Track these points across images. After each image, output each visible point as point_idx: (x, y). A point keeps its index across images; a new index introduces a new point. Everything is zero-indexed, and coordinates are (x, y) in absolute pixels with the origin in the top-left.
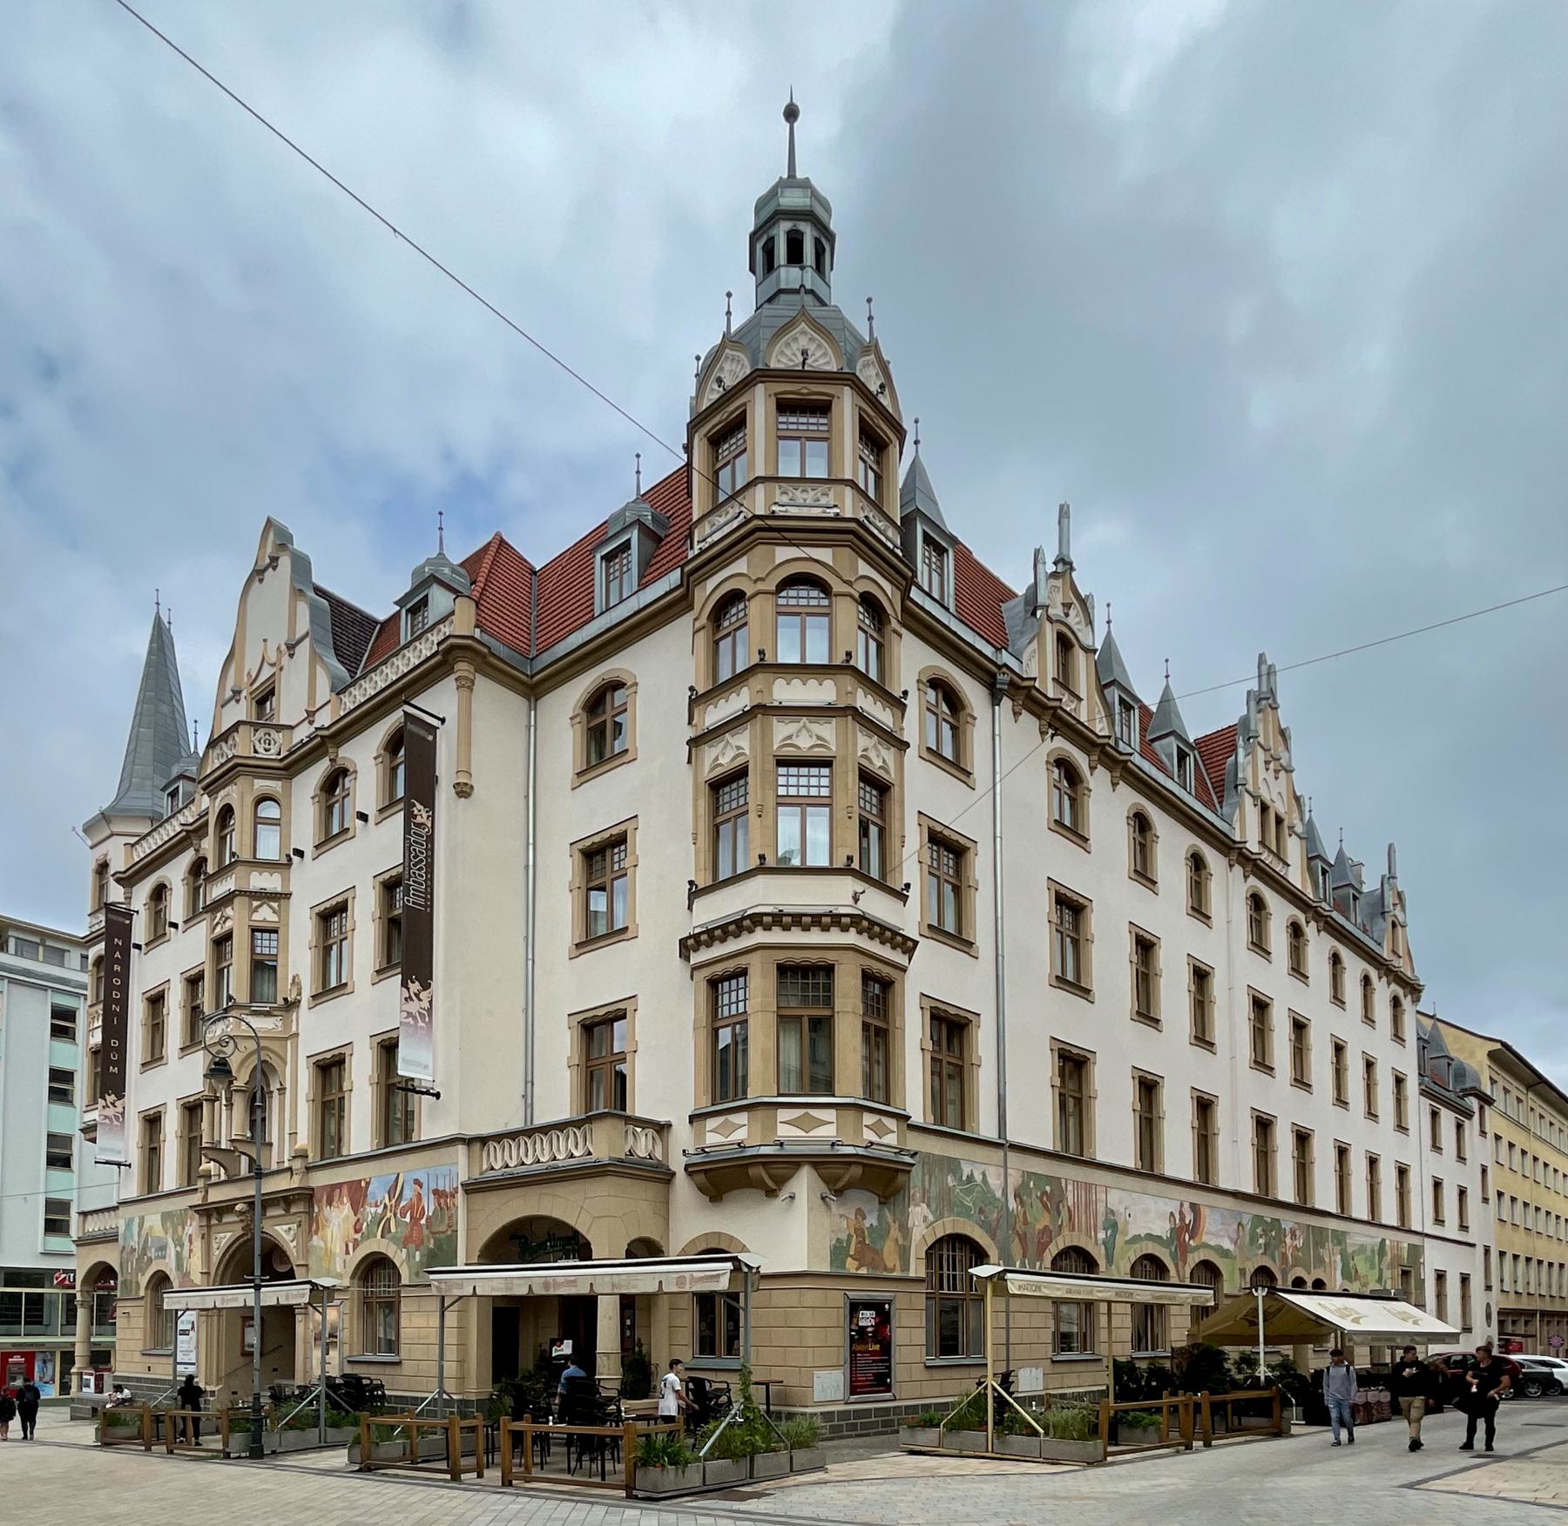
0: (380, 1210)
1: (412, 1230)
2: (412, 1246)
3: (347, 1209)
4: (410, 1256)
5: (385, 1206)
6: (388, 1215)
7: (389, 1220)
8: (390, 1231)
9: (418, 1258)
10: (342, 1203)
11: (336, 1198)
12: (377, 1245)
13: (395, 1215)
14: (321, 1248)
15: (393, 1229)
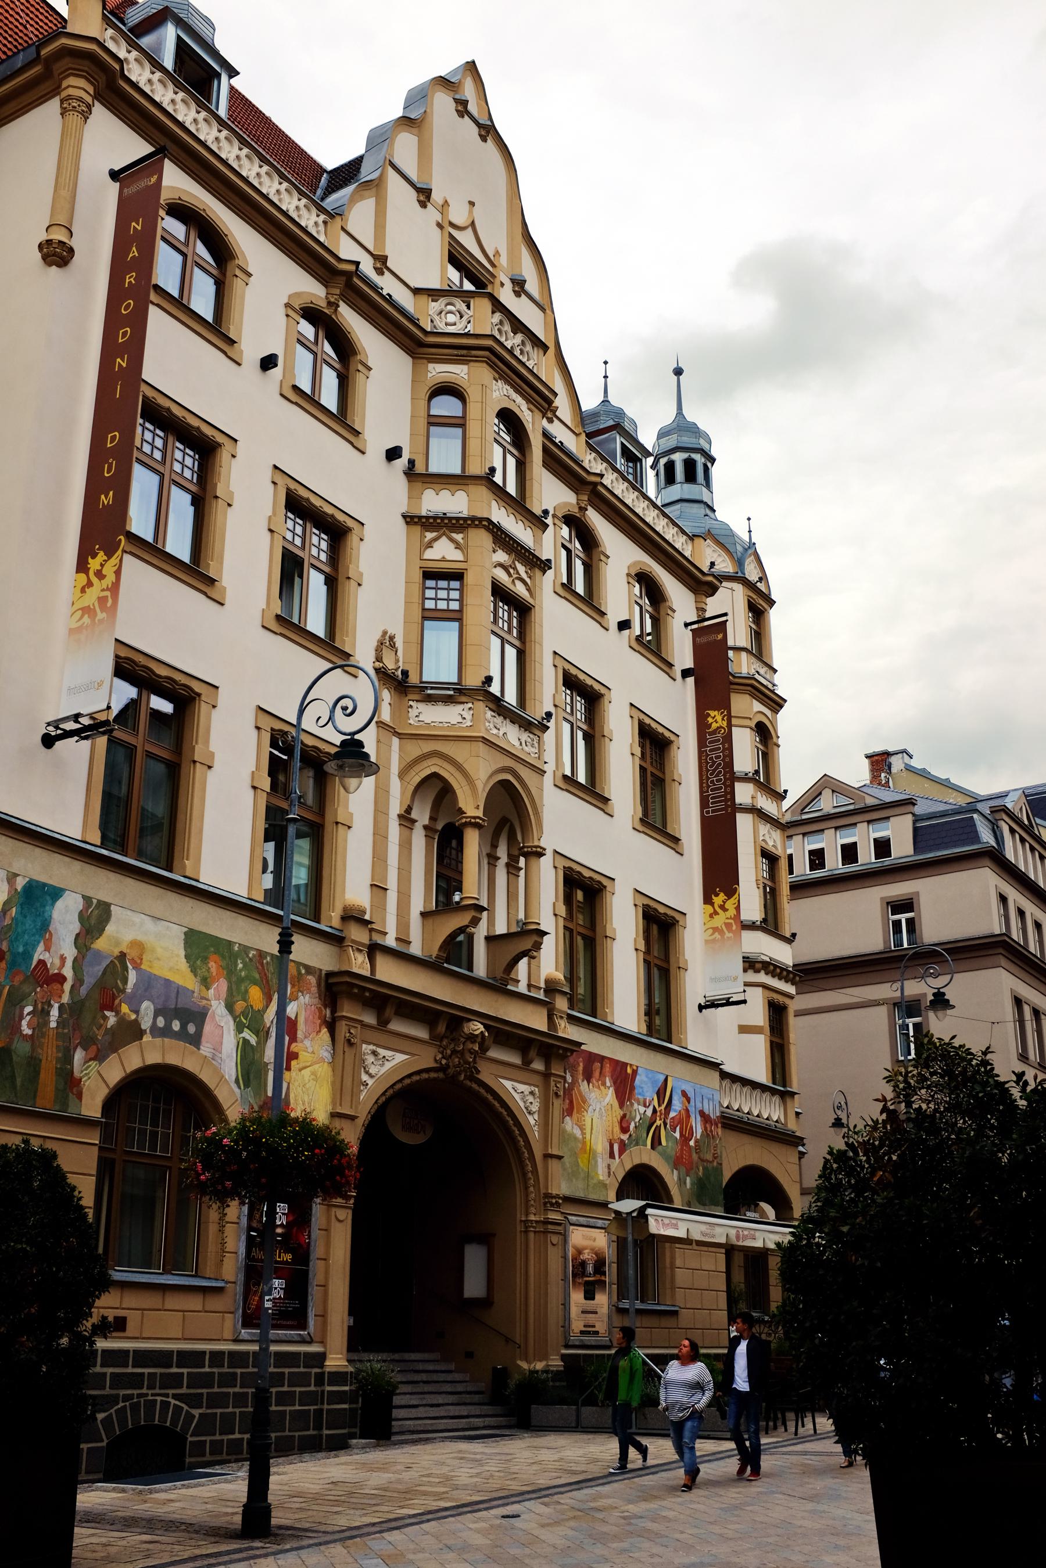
0: (649, 1112)
1: (682, 1150)
2: (683, 1170)
3: (609, 1095)
4: (681, 1182)
5: (655, 1111)
6: (658, 1122)
7: (658, 1128)
8: (660, 1143)
9: (688, 1185)
10: (604, 1084)
11: (597, 1074)
12: (644, 1155)
13: (665, 1124)
14: (576, 1138)
15: (664, 1143)
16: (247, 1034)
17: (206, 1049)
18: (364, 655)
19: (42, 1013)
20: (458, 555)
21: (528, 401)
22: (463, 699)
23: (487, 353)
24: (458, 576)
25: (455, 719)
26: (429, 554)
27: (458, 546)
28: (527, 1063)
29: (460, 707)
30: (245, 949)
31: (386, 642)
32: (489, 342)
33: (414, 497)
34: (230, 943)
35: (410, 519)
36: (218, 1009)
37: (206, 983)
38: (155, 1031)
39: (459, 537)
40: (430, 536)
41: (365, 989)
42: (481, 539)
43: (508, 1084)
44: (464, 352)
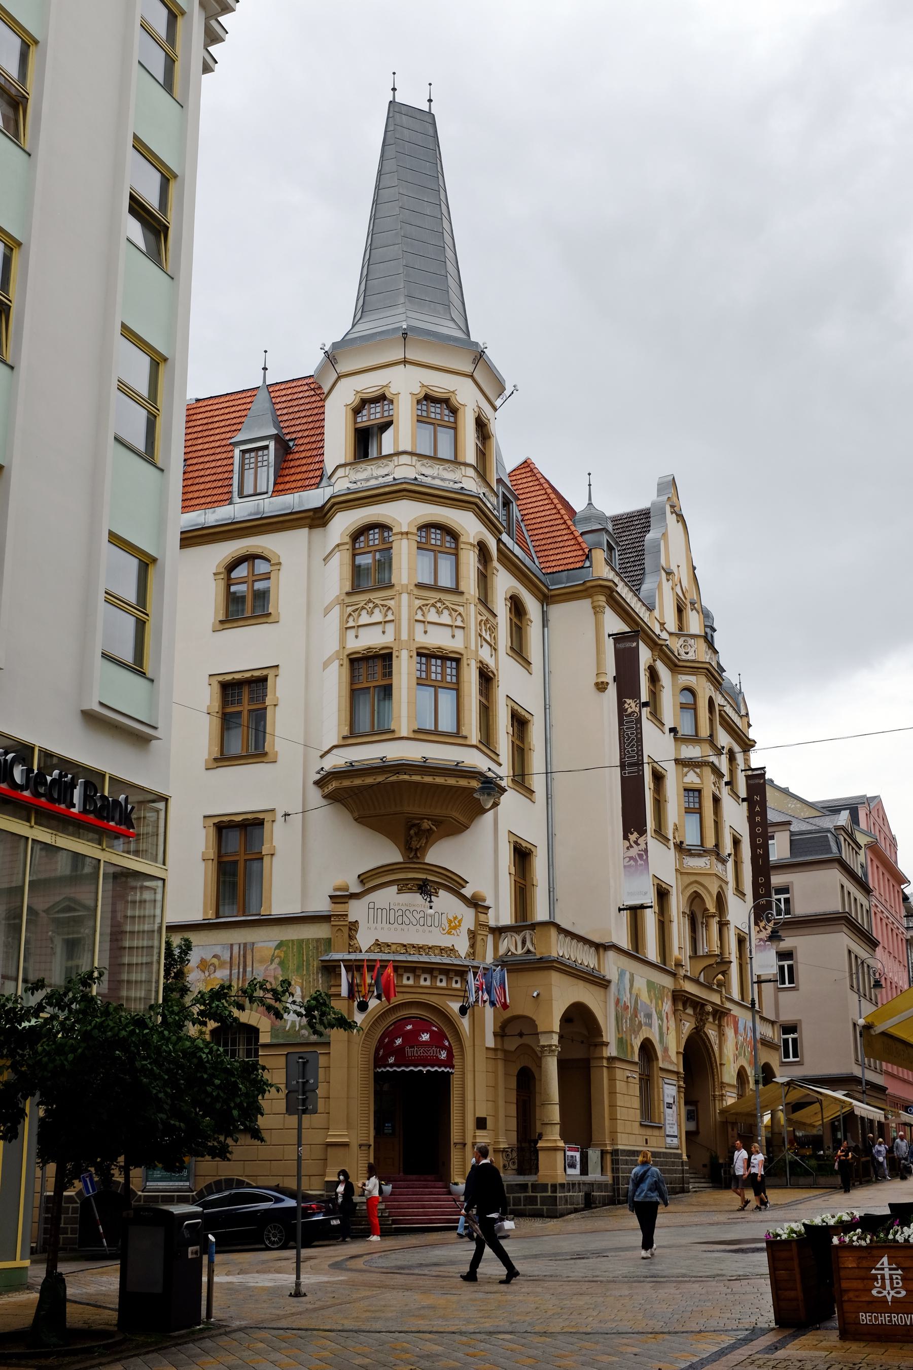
16: (660, 1022)
17: (653, 1030)
18: (671, 837)
19: (626, 1022)
20: (697, 780)
21: (714, 686)
22: (706, 855)
23: (705, 671)
24: (699, 791)
25: (703, 865)
26: (686, 780)
27: (698, 775)
28: (714, 1020)
29: (705, 858)
30: (657, 984)
31: (676, 829)
32: (707, 666)
33: (677, 750)
34: (654, 983)
35: (677, 761)
36: (654, 1012)
37: (651, 1002)
38: (646, 1024)
39: (698, 770)
40: (686, 770)
41: (685, 996)
42: (707, 771)
43: (710, 1031)
44: (695, 670)
